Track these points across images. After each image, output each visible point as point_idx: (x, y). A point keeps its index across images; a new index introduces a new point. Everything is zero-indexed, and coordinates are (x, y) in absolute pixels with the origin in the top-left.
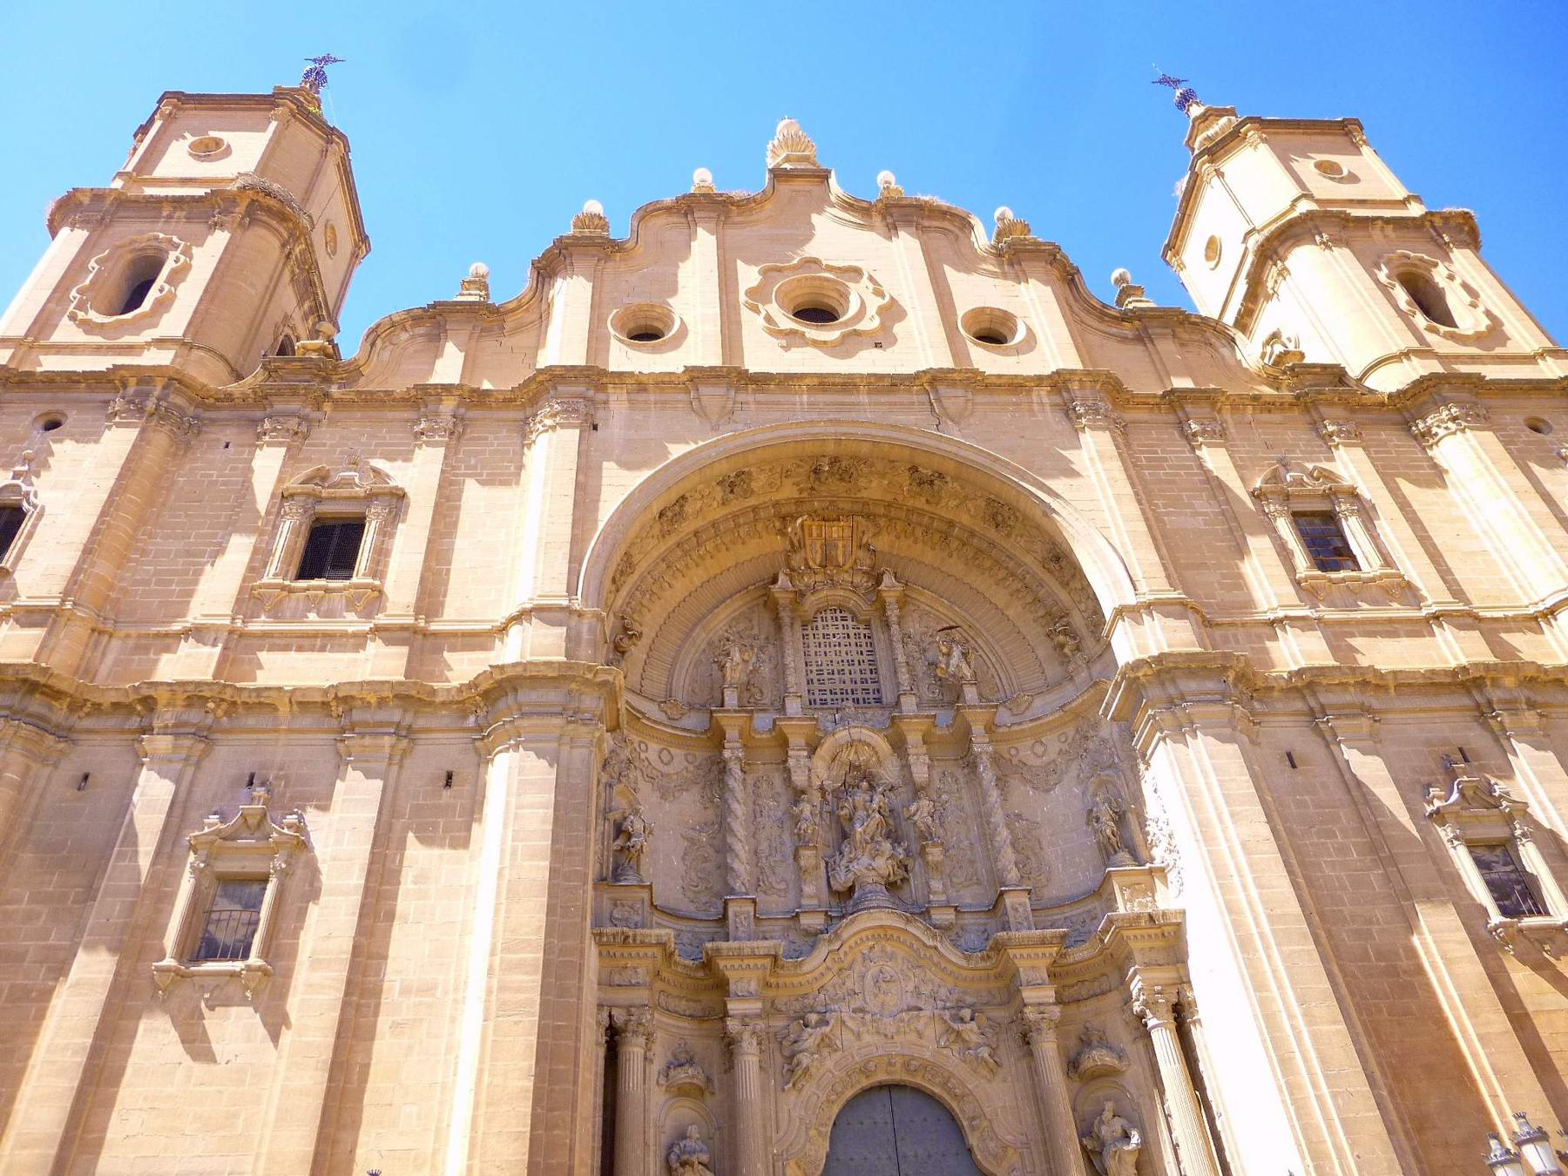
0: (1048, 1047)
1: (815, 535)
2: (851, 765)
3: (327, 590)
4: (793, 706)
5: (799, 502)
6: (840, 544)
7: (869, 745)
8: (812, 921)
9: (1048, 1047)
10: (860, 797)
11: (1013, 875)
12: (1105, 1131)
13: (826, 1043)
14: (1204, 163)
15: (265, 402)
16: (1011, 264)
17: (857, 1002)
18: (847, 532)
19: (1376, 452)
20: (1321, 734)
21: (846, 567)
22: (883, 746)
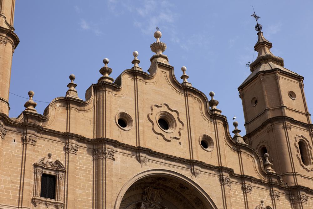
1: (151, 192)
3: (50, 202)
5: (151, 183)
6: (156, 195)
14: (261, 75)
15: (25, 127)
19: (281, 203)
21: (156, 202)
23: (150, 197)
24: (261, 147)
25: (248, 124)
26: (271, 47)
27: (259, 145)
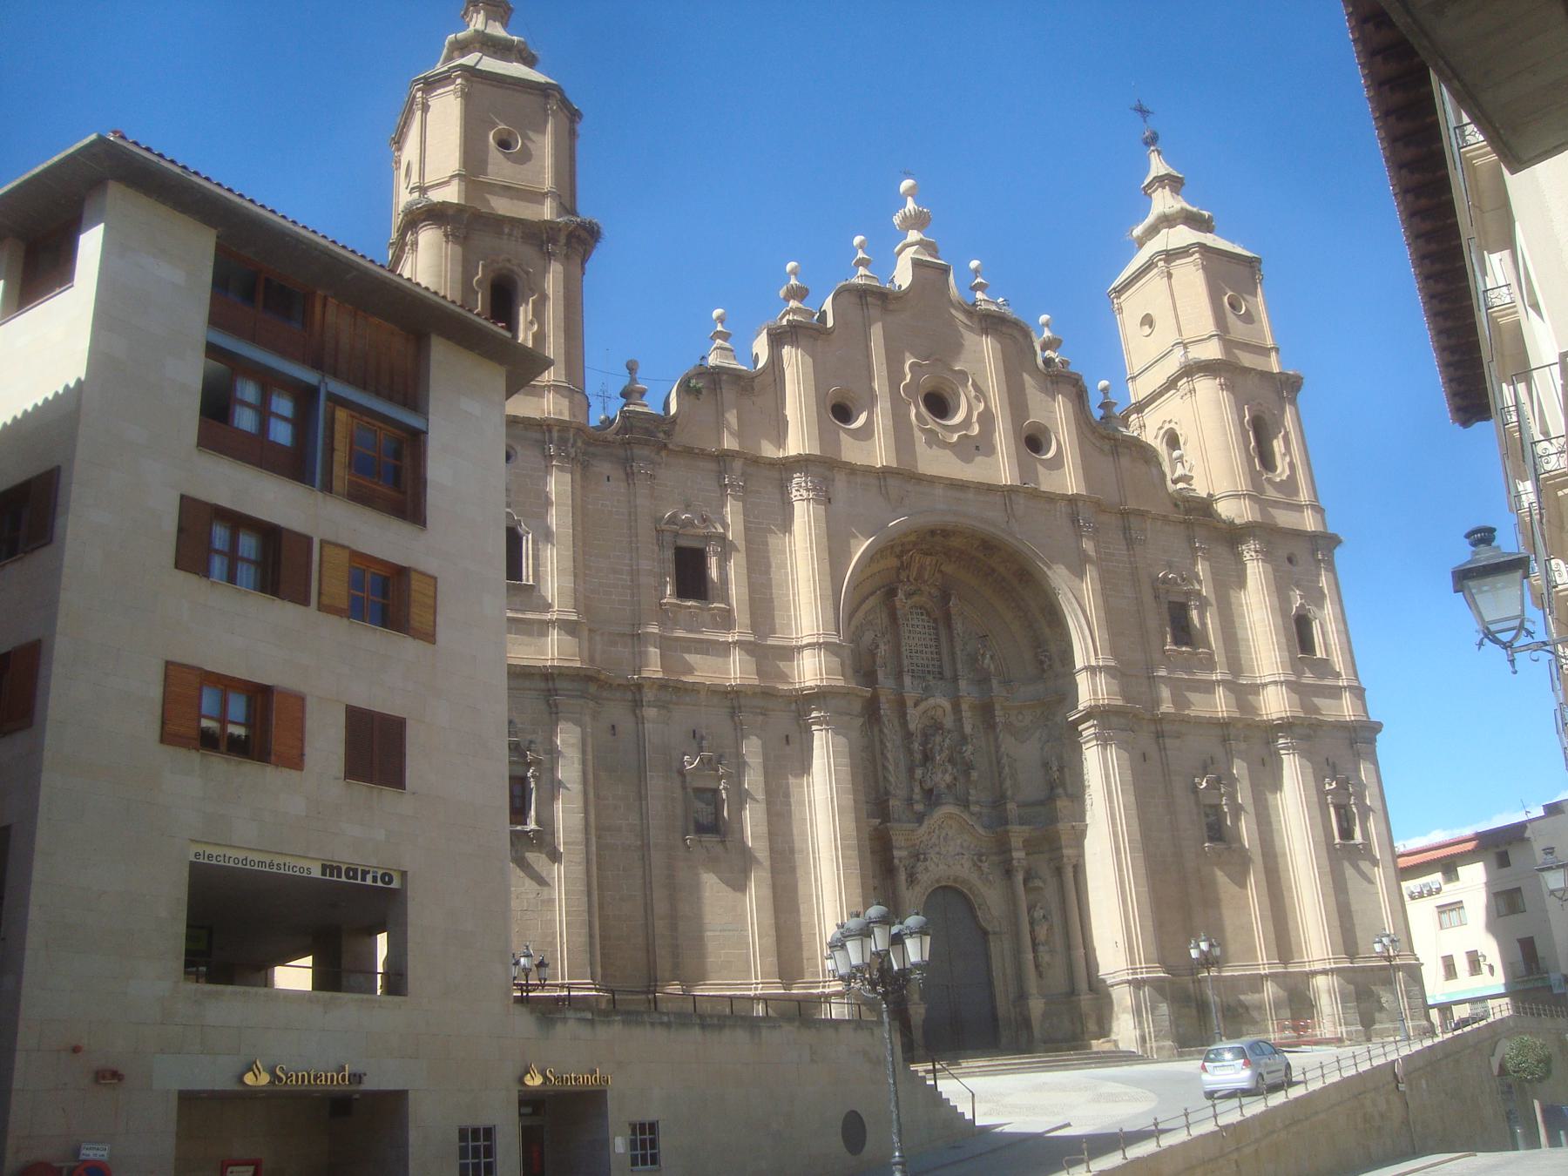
0: (1020, 877)
2: (932, 718)
4: (907, 680)
6: (928, 568)
7: (942, 707)
8: (919, 807)
9: (1020, 877)
10: (938, 739)
11: (1009, 793)
12: (1036, 915)
13: (926, 869)
14: (1160, 260)
16: (1052, 383)
17: (937, 849)
18: (934, 562)
20: (1158, 744)
21: (929, 583)
22: (947, 705)
23: (914, 574)
24: (1166, 433)
25: (1135, 377)
26: (1182, 184)
27: (1161, 428)
